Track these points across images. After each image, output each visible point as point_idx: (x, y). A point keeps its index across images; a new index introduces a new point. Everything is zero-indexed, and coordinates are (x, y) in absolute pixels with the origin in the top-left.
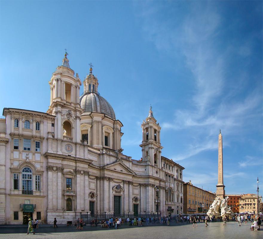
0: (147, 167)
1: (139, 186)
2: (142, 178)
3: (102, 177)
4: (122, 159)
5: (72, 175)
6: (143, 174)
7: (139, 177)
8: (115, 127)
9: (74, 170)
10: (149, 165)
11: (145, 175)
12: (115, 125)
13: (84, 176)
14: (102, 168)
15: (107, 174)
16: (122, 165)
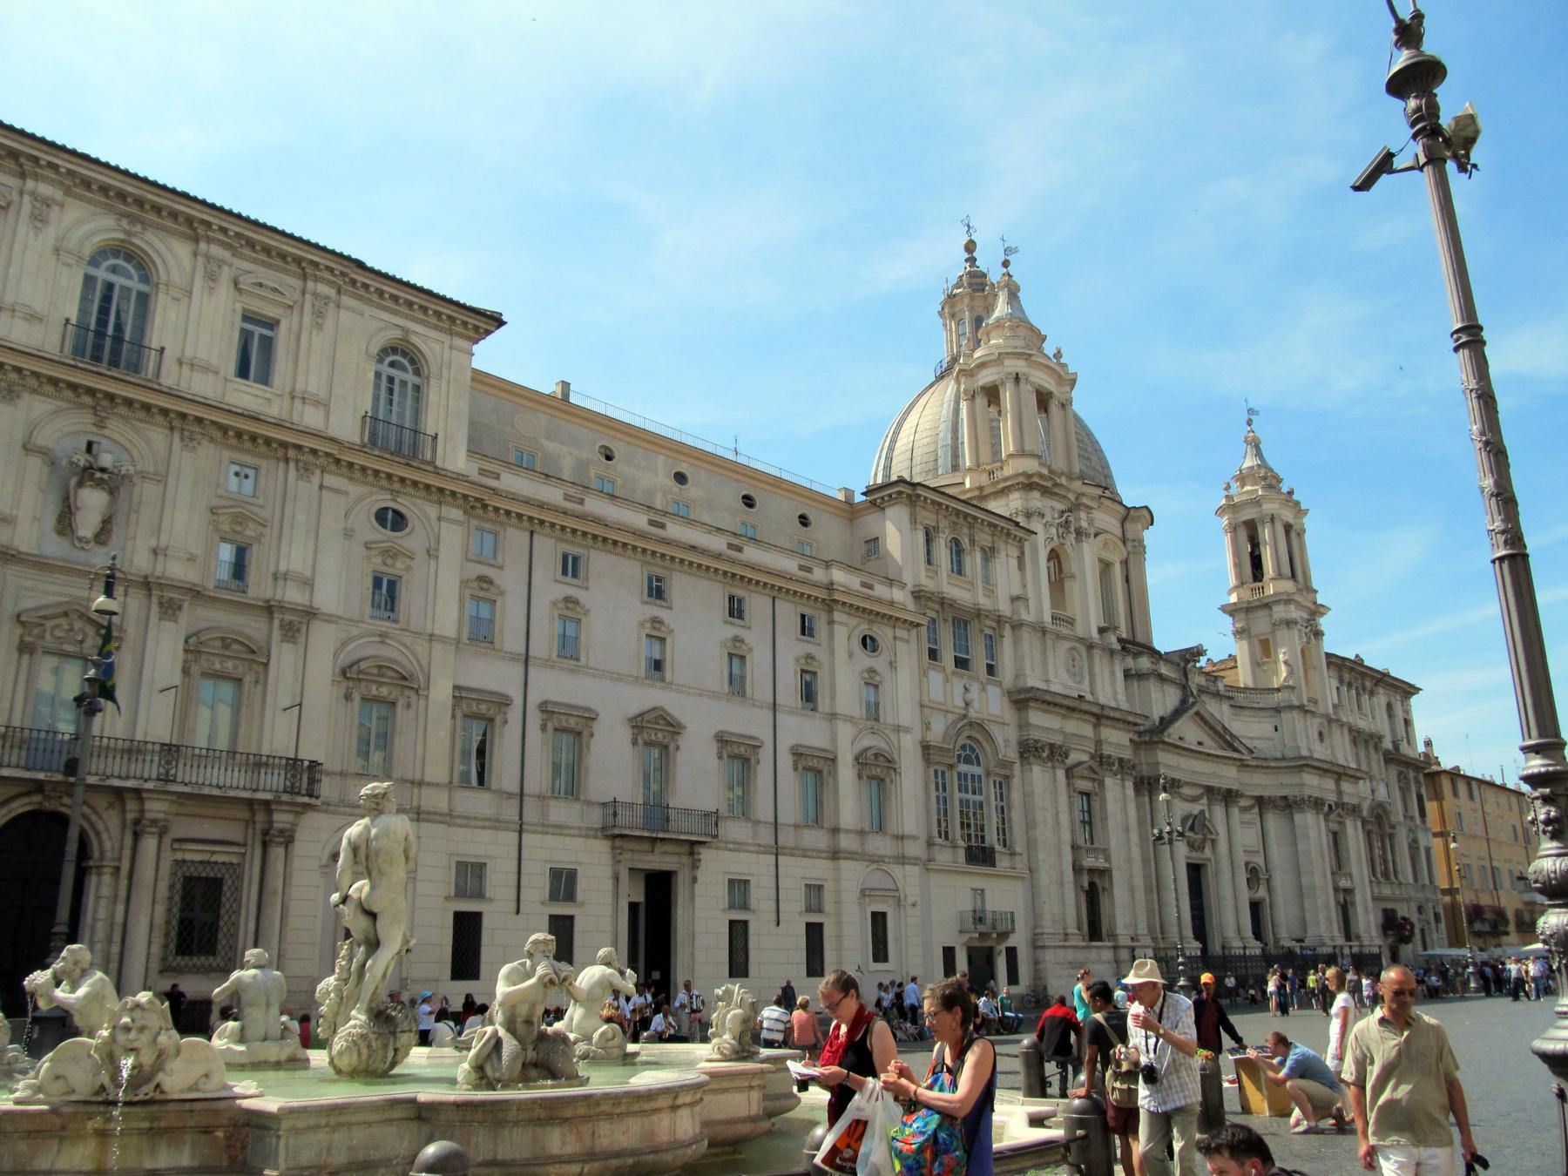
0: (1286, 717)
1: (1256, 810)
2: (1268, 767)
3: (1149, 778)
4: (1202, 690)
5: (1094, 780)
6: (1267, 748)
7: (1257, 767)
8: (1129, 535)
9: (1092, 757)
10: (1291, 707)
11: (1279, 755)
12: (1128, 526)
13: (1123, 779)
14: (1152, 735)
15: (1168, 763)
16: (1202, 718)
